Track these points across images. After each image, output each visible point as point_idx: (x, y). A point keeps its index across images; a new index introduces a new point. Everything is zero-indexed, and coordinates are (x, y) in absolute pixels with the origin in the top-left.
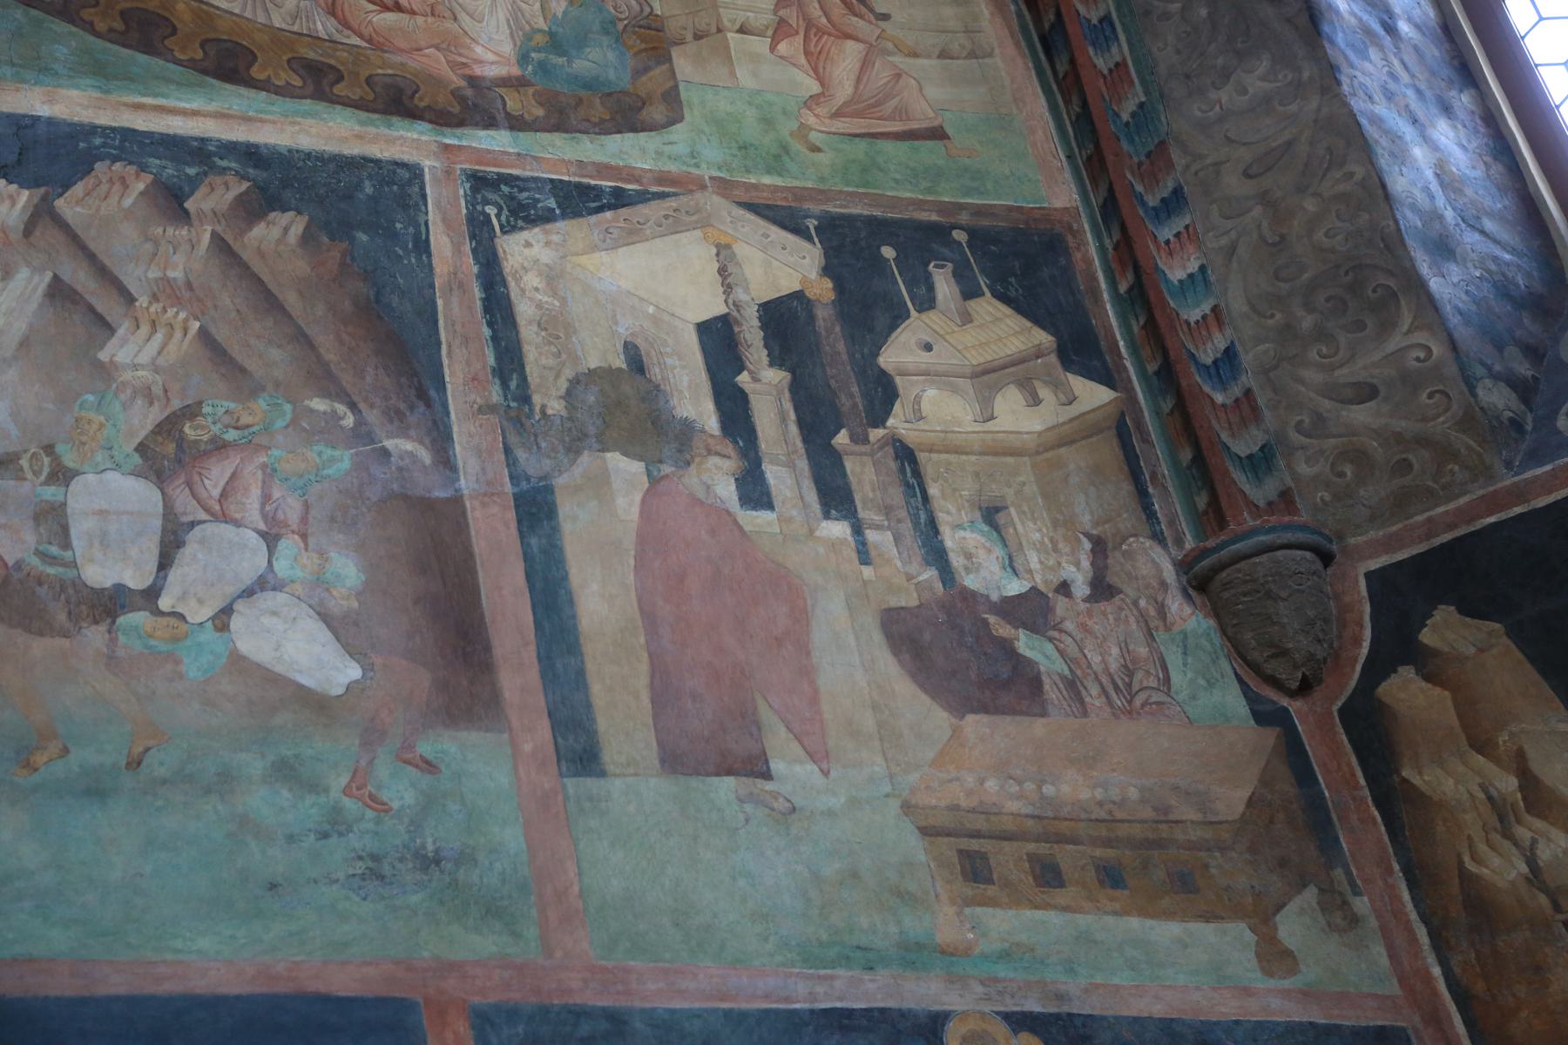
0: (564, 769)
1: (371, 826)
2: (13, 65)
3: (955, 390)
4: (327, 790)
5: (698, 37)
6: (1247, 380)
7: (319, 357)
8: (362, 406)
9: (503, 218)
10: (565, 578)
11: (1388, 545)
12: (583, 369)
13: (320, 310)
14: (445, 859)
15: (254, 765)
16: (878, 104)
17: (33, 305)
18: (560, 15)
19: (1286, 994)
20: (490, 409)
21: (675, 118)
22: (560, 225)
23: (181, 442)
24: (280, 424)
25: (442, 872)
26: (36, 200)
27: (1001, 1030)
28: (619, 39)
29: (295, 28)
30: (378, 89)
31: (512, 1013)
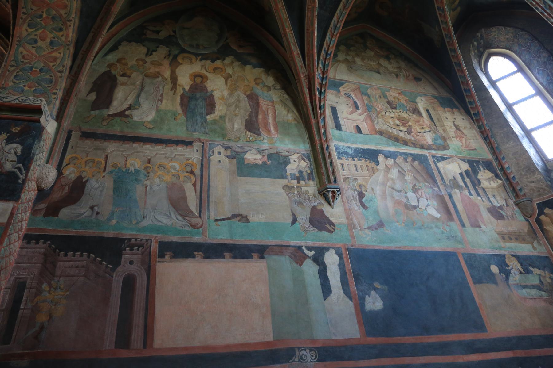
3: (486, 181)
5: (448, 138)
6: (517, 180)
11: (538, 200)
15: (434, 226)
19: (536, 252)
20: (442, 184)
21: (449, 149)
22: (442, 162)
27: (511, 256)
31: (465, 254)
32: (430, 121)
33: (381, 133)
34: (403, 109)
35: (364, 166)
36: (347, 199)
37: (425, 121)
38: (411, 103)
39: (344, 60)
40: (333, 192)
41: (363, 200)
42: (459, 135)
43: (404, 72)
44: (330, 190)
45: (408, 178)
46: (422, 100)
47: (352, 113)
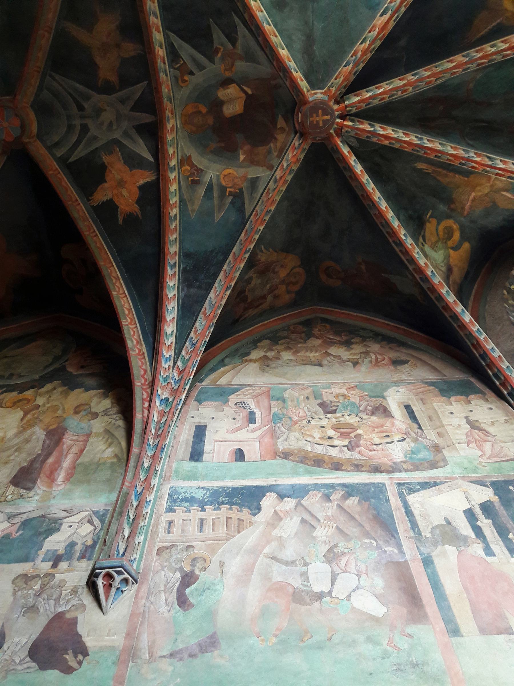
0: (450, 635)
1: (396, 655)
2: (291, 474)
4: (382, 645)
5: (448, 446)
7: (365, 529)
8: (378, 540)
9: (407, 492)
10: (440, 580)
12: (434, 525)
13: (364, 518)
14: (419, 664)
15: (361, 638)
16: (498, 455)
17: (298, 525)
18: (413, 446)
22: (422, 492)
23: (334, 554)
24: (358, 547)
25: (419, 668)
26: (297, 501)
28: (428, 449)
29: (352, 458)
30: (372, 468)
32: (409, 421)
33: (286, 455)
34: (351, 411)
35: (223, 519)
36: (149, 591)
37: (397, 423)
38: (372, 399)
39: (260, 358)
40: (109, 576)
41: (187, 591)
42: (477, 437)
43: (374, 357)
44: (101, 573)
45: (320, 533)
46: (398, 391)
47: (238, 429)
